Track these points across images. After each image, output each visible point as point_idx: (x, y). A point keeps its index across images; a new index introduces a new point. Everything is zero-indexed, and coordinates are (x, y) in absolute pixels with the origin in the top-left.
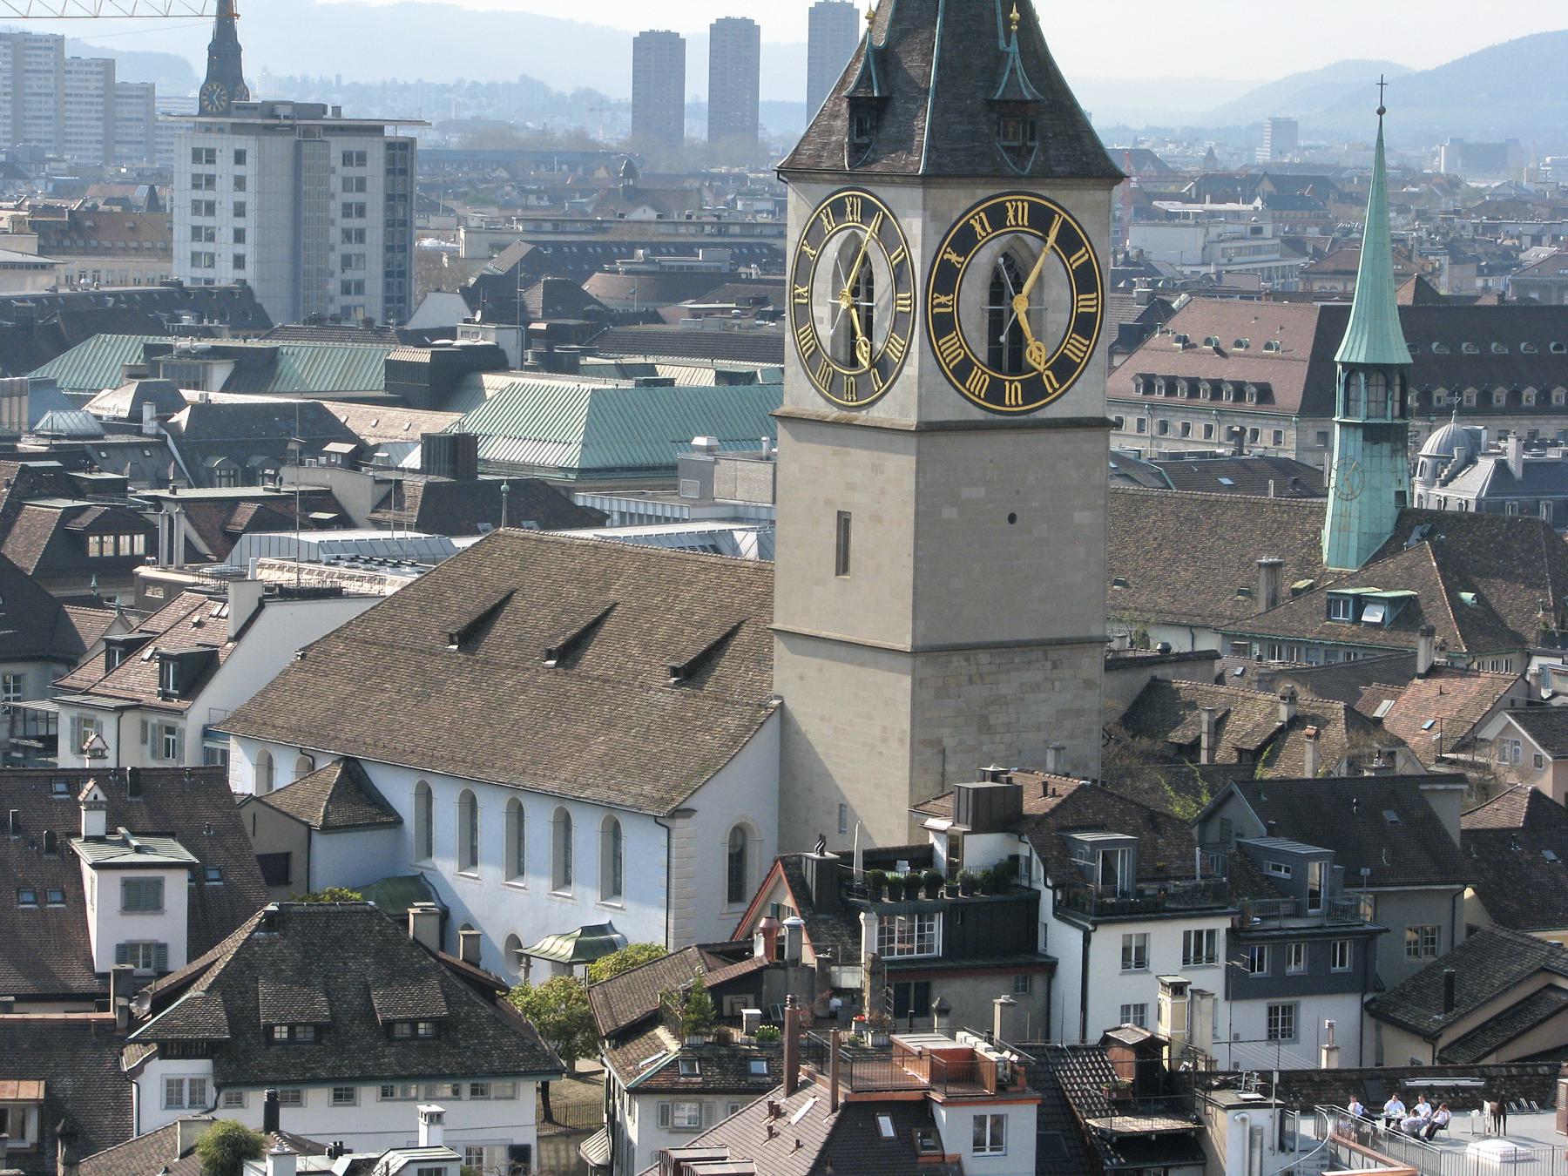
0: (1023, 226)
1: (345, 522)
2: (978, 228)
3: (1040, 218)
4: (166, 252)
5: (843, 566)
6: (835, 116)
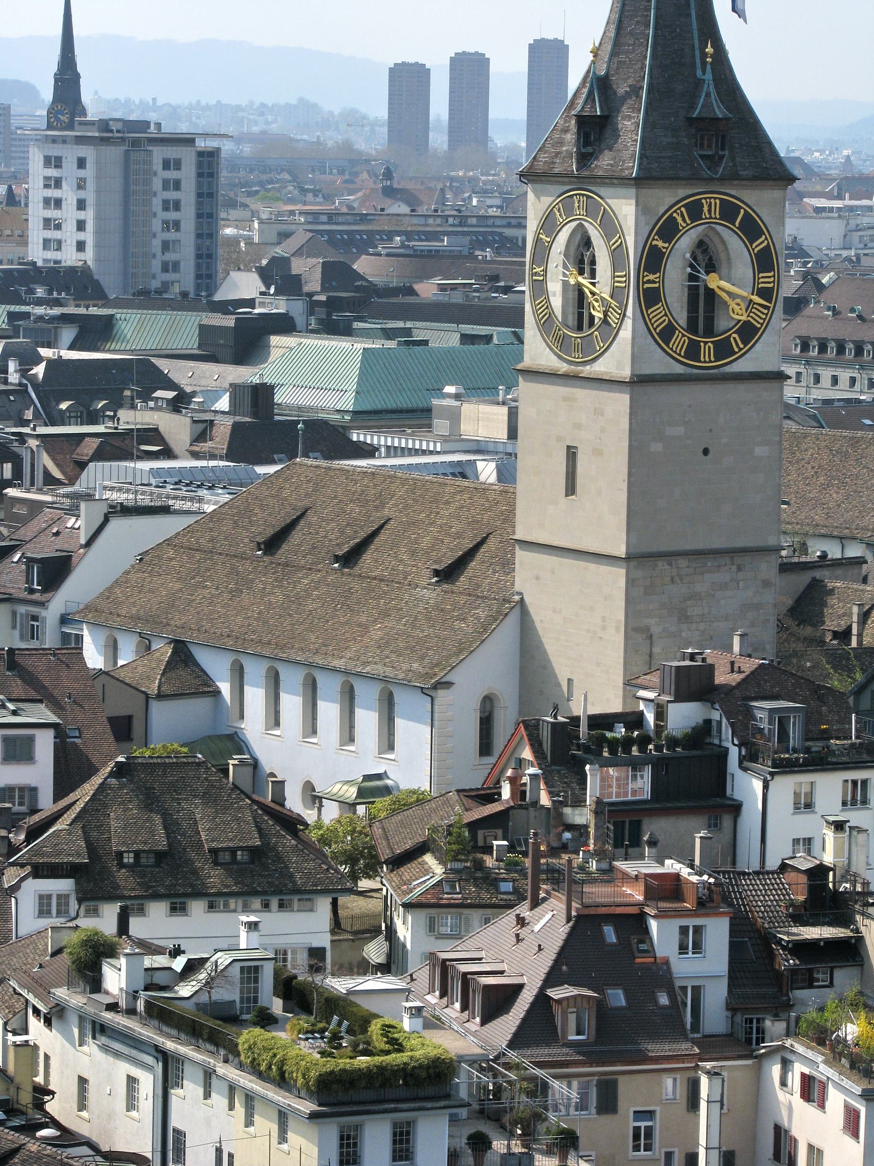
0: (716, 218)
1: (167, 453)
2: (679, 220)
3: (729, 212)
4: (22, 238)
5: (571, 489)
6: (566, 131)
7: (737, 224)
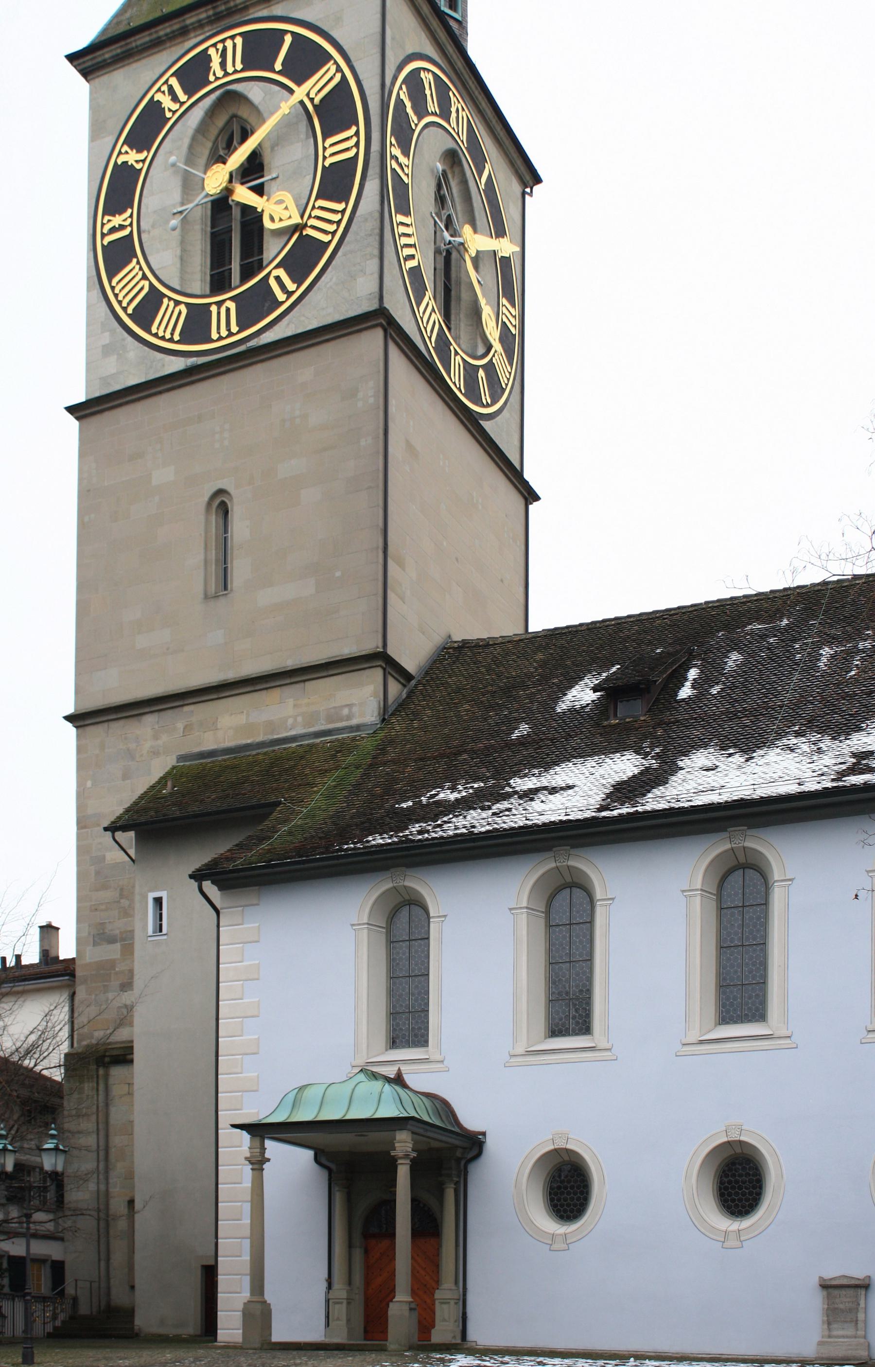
2: (166, 102)
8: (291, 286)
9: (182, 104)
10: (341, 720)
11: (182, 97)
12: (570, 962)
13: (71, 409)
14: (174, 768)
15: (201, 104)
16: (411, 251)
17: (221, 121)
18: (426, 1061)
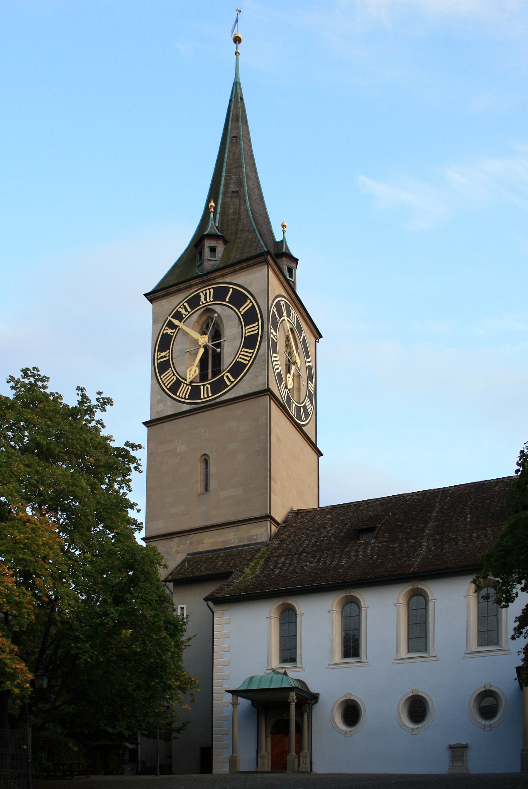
0: (210, 301)
2: (183, 311)
7: (227, 300)
8: (232, 380)
9: (189, 312)
10: (253, 540)
11: (189, 310)
12: (351, 630)
13: (145, 423)
14: (186, 558)
15: (197, 313)
16: (277, 366)
17: (204, 318)
18: (296, 667)
